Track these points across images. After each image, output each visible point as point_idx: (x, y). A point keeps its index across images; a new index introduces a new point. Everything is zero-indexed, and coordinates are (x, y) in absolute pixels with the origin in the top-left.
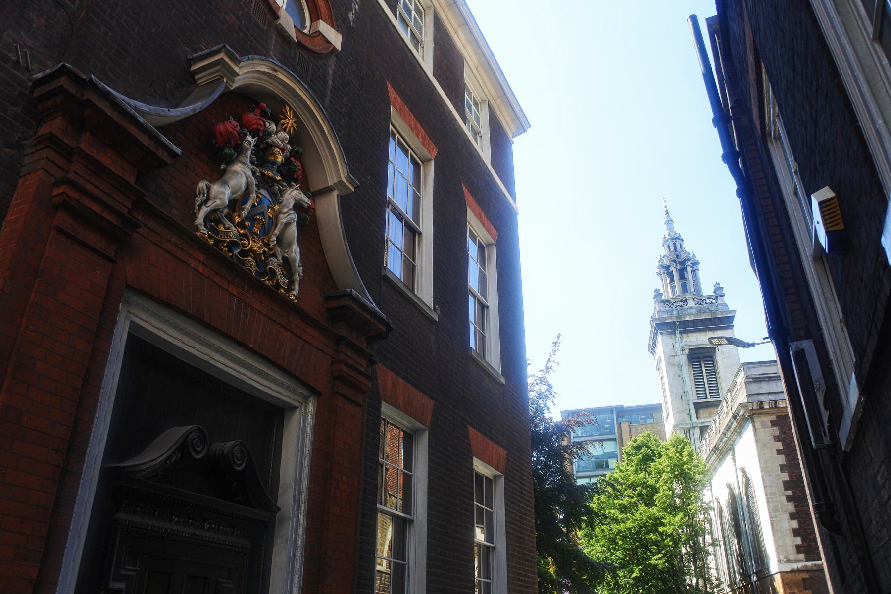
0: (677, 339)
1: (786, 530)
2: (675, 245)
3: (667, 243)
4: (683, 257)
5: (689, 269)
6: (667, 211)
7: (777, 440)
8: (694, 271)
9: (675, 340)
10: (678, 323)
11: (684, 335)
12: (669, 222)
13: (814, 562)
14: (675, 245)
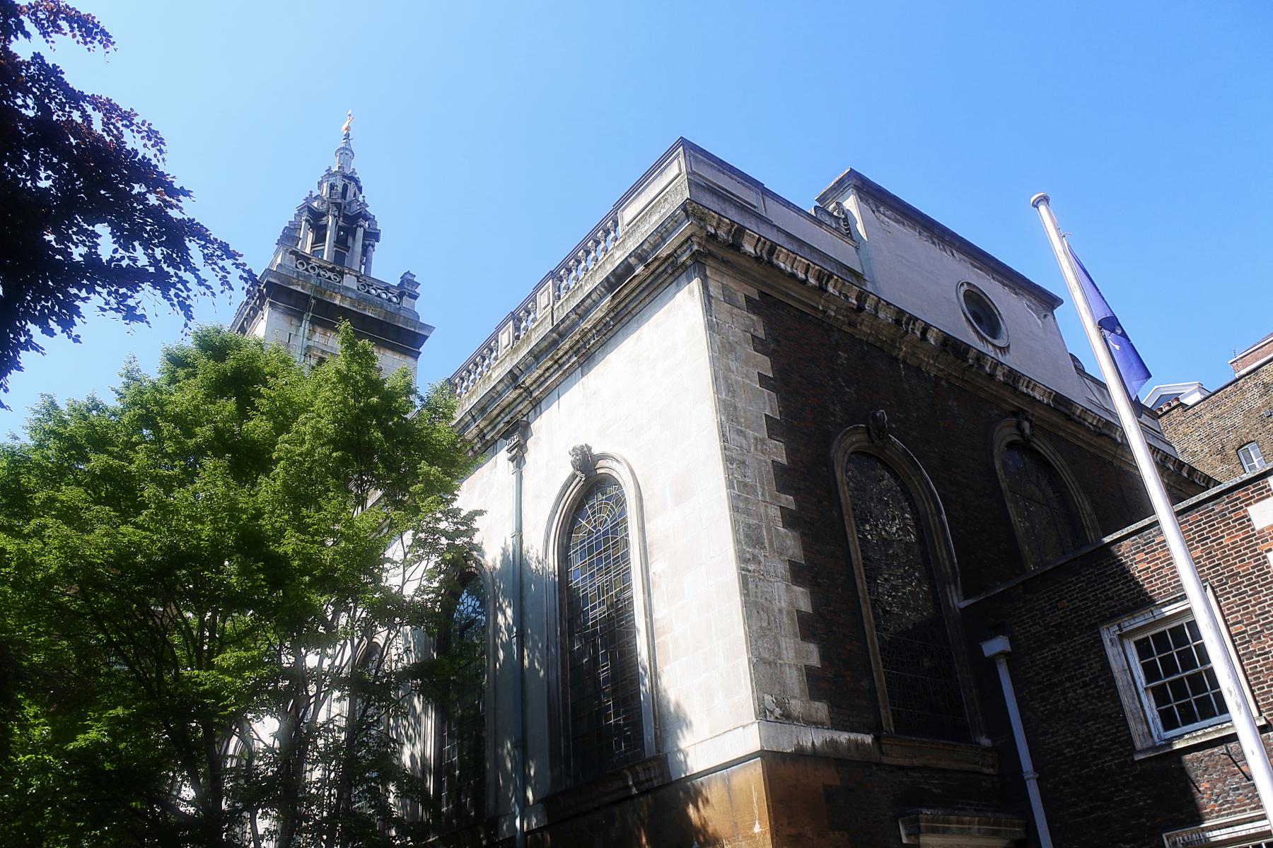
0: (302, 329)
1: (780, 611)
2: (345, 188)
3: (332, 180)
4: (355, 208)
5: (360, 232)
6: (347, 136)
7: (760, 347)
8: (365, 250)
9: (297, 330)
10: (313, 301)
11: (319, 330)
12: (346, 152)
13: (853, 736)
14: (345, 188)
